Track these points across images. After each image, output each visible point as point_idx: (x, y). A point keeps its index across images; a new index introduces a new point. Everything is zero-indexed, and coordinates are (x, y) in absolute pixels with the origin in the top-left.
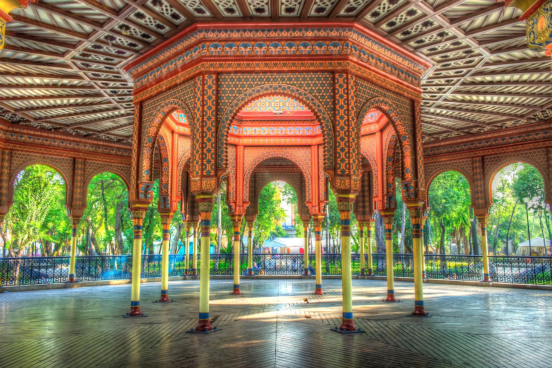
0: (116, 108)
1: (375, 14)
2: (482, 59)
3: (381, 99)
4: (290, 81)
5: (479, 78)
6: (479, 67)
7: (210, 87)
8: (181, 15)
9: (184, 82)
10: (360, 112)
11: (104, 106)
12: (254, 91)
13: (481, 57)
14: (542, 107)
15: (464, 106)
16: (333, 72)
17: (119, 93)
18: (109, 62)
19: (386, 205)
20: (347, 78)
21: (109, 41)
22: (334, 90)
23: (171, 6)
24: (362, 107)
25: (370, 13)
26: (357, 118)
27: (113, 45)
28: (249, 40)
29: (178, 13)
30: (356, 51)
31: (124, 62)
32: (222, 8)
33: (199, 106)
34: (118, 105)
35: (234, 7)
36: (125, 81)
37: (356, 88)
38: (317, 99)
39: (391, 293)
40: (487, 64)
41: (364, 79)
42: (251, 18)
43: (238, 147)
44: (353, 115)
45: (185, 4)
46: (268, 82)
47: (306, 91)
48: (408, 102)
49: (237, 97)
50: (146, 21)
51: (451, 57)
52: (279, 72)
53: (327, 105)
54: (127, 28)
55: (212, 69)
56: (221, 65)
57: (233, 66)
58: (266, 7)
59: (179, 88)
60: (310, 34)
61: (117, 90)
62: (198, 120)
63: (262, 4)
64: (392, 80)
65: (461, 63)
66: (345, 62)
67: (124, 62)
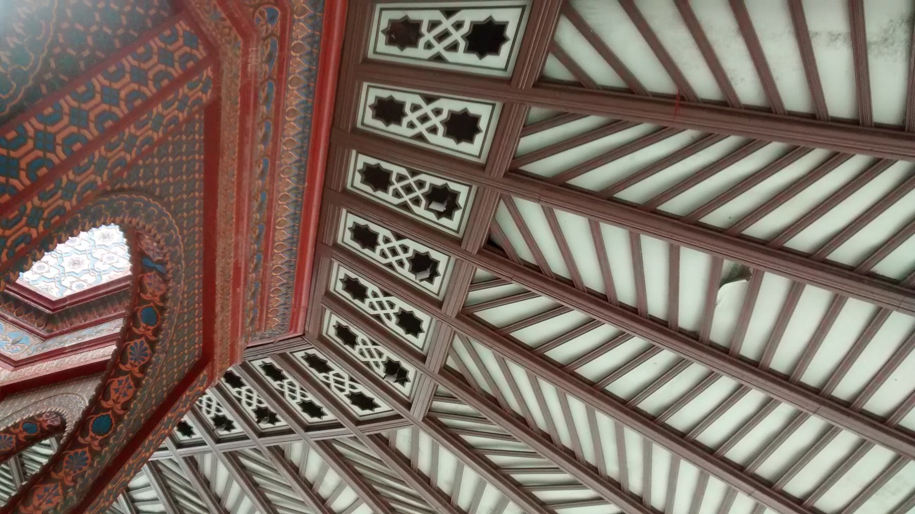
2: (398, 417)
10: (122, 190)
13: (400, 409)
20: (200, 66)
40: (383, 443)
66: (234, 32)
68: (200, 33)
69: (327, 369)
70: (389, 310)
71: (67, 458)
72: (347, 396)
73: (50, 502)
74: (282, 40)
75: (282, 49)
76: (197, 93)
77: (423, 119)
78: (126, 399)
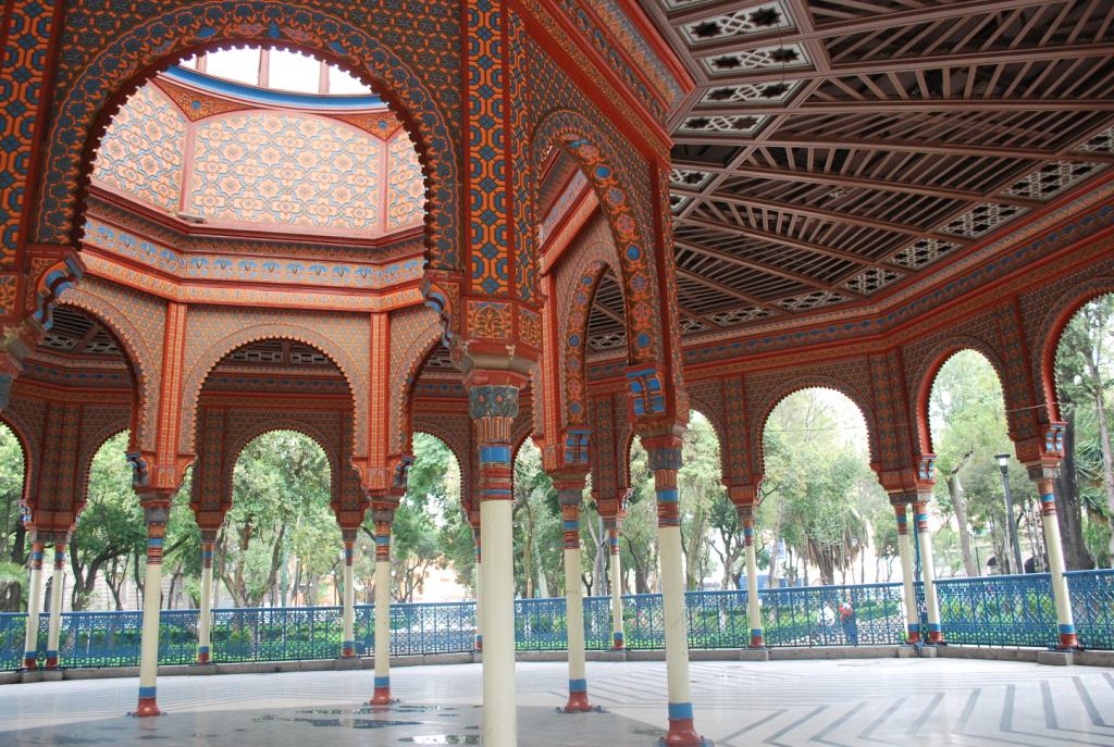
10: (535, 128)
19: (566, 456)
22: (462, 45)
24: (541, 119)
39: (578, 690)
43: (173, 306)
70: (744, 23)
71: (632, 286)
72: (761, 96)
73: (646, 314)
78: (633, 228)
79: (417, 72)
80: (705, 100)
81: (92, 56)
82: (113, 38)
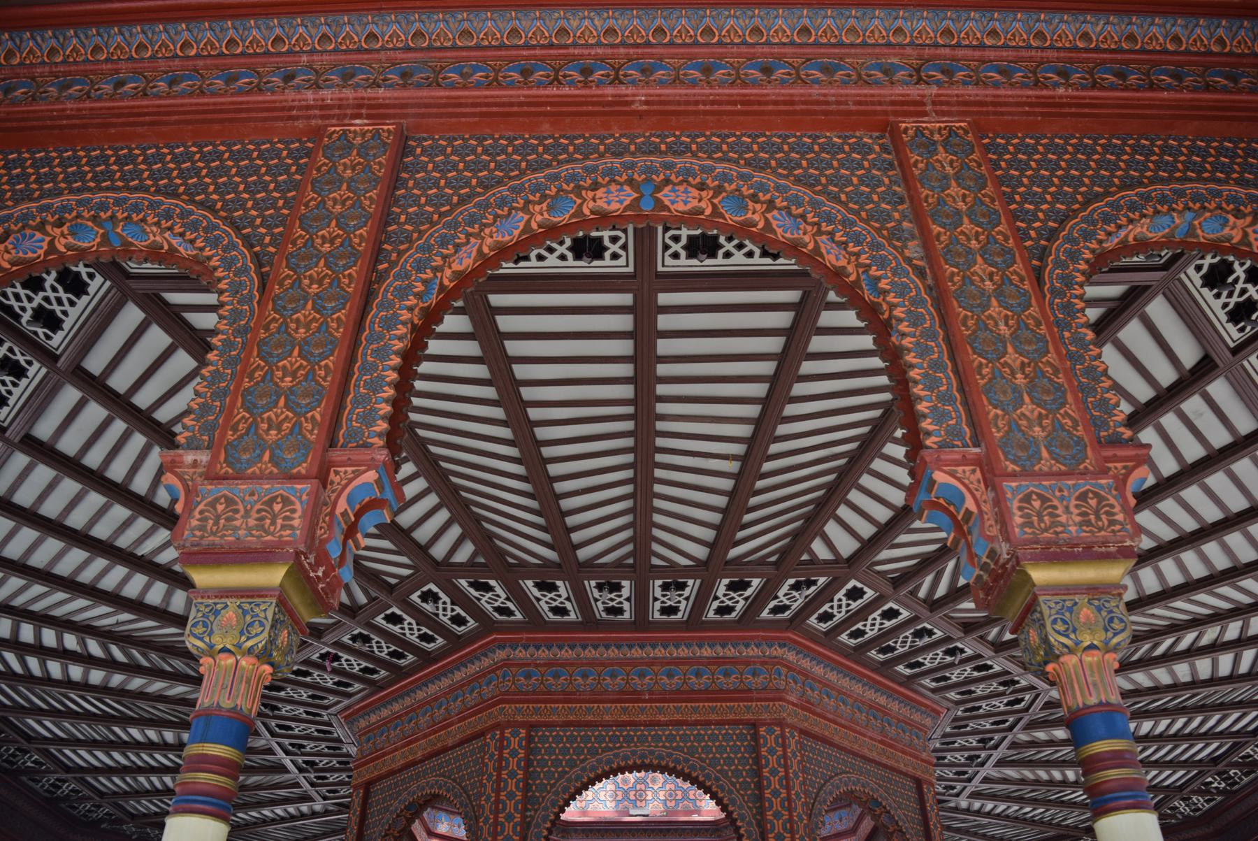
0: (306, 798)
1: (826, 617)
3: (854, 777)
4: (671, 742)
5: (1041, 735)
6: (1036, 712)
7: (514, 753)
8: (468, 618)
9: (461, 743)
11: (282, 792)
12: (599, 762)
13: (1034, 693)
14: (1181, 788)
15: (1026, 791)
16: (754, 725)
17: (321, 765)
18: (317, 701)
20: (783, 736)
21: (327, 663)
22: (757, 760)
23: (453, 603)
25: (816, 615)
26: (810, 816)
27: (335, 671)
28: (592, 663)
29: (463, 614)
30: (796, 682)
31: (346, 702)
32: (546, 607)
33: (489, 790)
34: (312, 792)
35: (568, 605)
36: (339, 740)
37: (802, 756)
38: (726, 777)
41: (815, 737)
42: (597, 625)
44: (799, 810)
45: (479, 600)
46: (628, 742)
47: (702, 760)
48: (910, 784)
49: (567, 773)
50: (403, 629)
51: (979, 692)
52: (646, 724)
53: (745, 790)
54: (366, 639)
55: (519, 718)
56: (537, 711)
57: (559, 713)
58: (626, 606)
59: (451, 755)
60: (707, 652)
61: (317, 759)
62: (487, 819)
63: (619, 600)
64: (871, 738)
65: (1000, 704)
67: (346, 702)
68: (769, 724)
69: (980, 707)
74: (790, 668)
75: (794, 670)
76: (793, 740)
77: (873, 626)
79: (733, 784)
80: (960, 713)
81: (544, 798)
82: (552, 786)
